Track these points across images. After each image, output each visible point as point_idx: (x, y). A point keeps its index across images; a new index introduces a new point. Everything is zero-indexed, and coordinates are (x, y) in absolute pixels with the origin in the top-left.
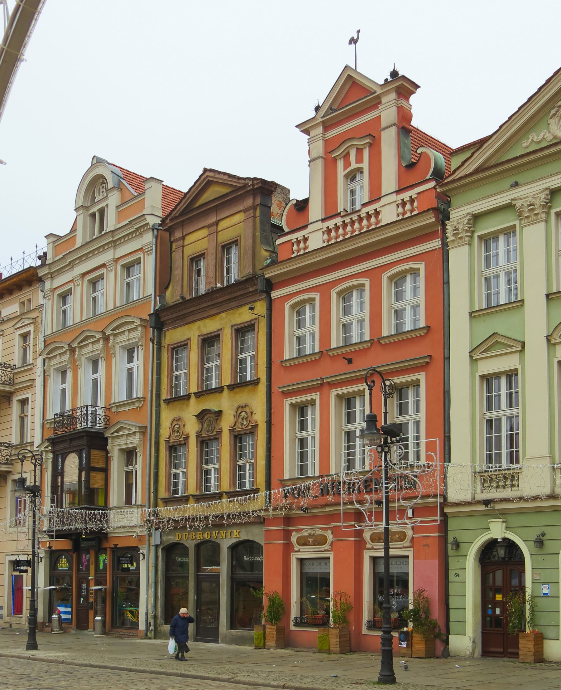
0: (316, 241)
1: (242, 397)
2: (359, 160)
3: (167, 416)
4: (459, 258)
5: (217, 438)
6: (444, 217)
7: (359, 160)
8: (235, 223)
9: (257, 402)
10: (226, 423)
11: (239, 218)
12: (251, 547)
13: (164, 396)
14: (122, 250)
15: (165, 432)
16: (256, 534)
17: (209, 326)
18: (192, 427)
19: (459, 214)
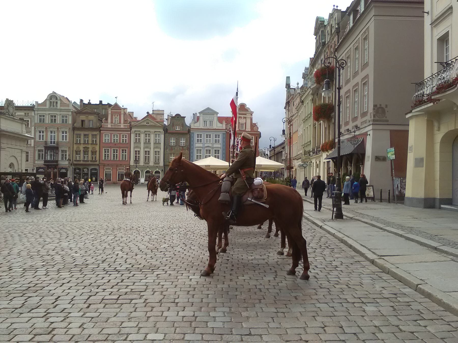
0: (109, 126)
1: (94, 146)
2: (117, 116)
3: (75, 146)
4: (133, 136)
5: (88, 152)
6: (131, 130)
7: (117, 116)
8: (92, 117)
9: (97, 148)
10: (90, 150)
11: (93, 117)
12: (96, 169)
13: (74, 142)
14: (61, 113)
15: (75, 149)
16: (97, 167)
17: (86, 133)
18: (82, 149)
19: (133, 130)
